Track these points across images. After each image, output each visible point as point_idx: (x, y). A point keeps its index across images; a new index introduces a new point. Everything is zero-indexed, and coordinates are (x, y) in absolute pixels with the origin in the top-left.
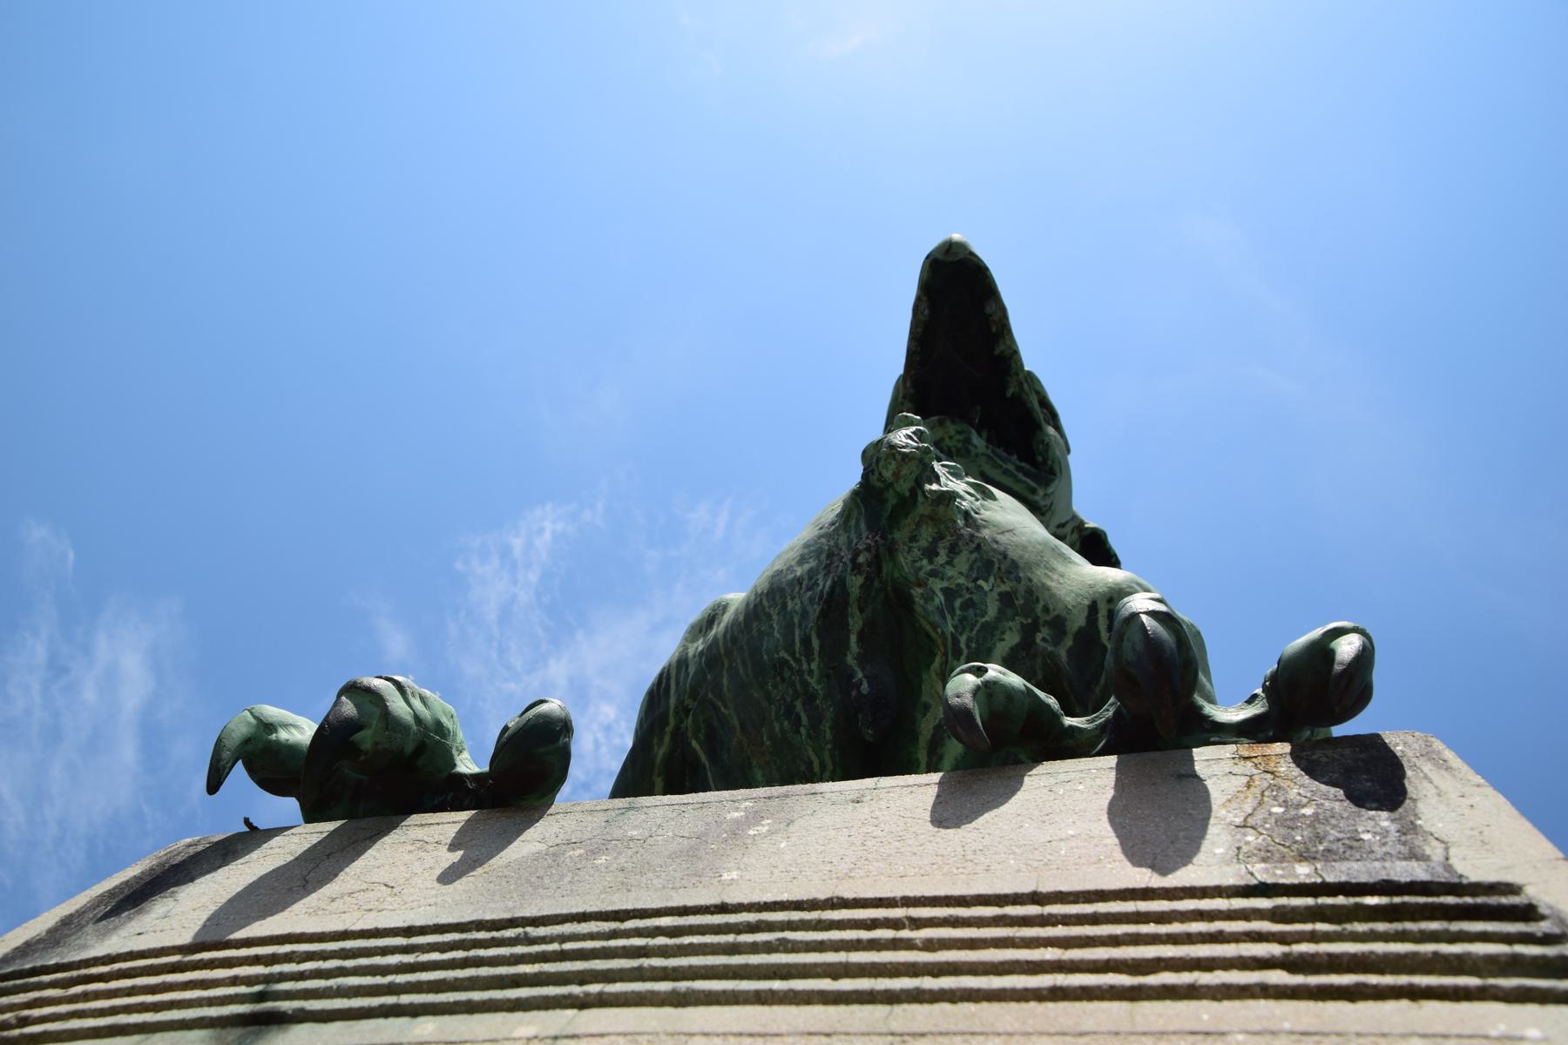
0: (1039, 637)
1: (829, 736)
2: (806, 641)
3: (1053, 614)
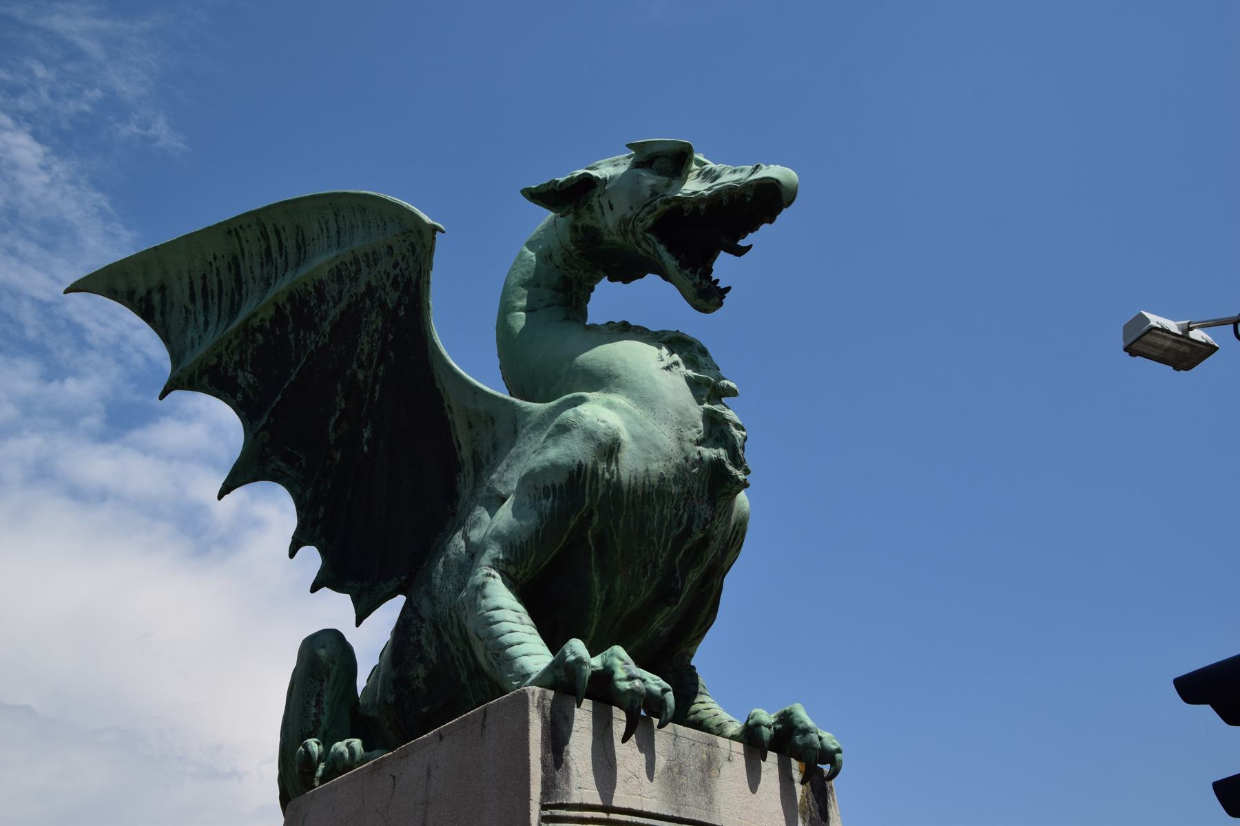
2: (666, 541)
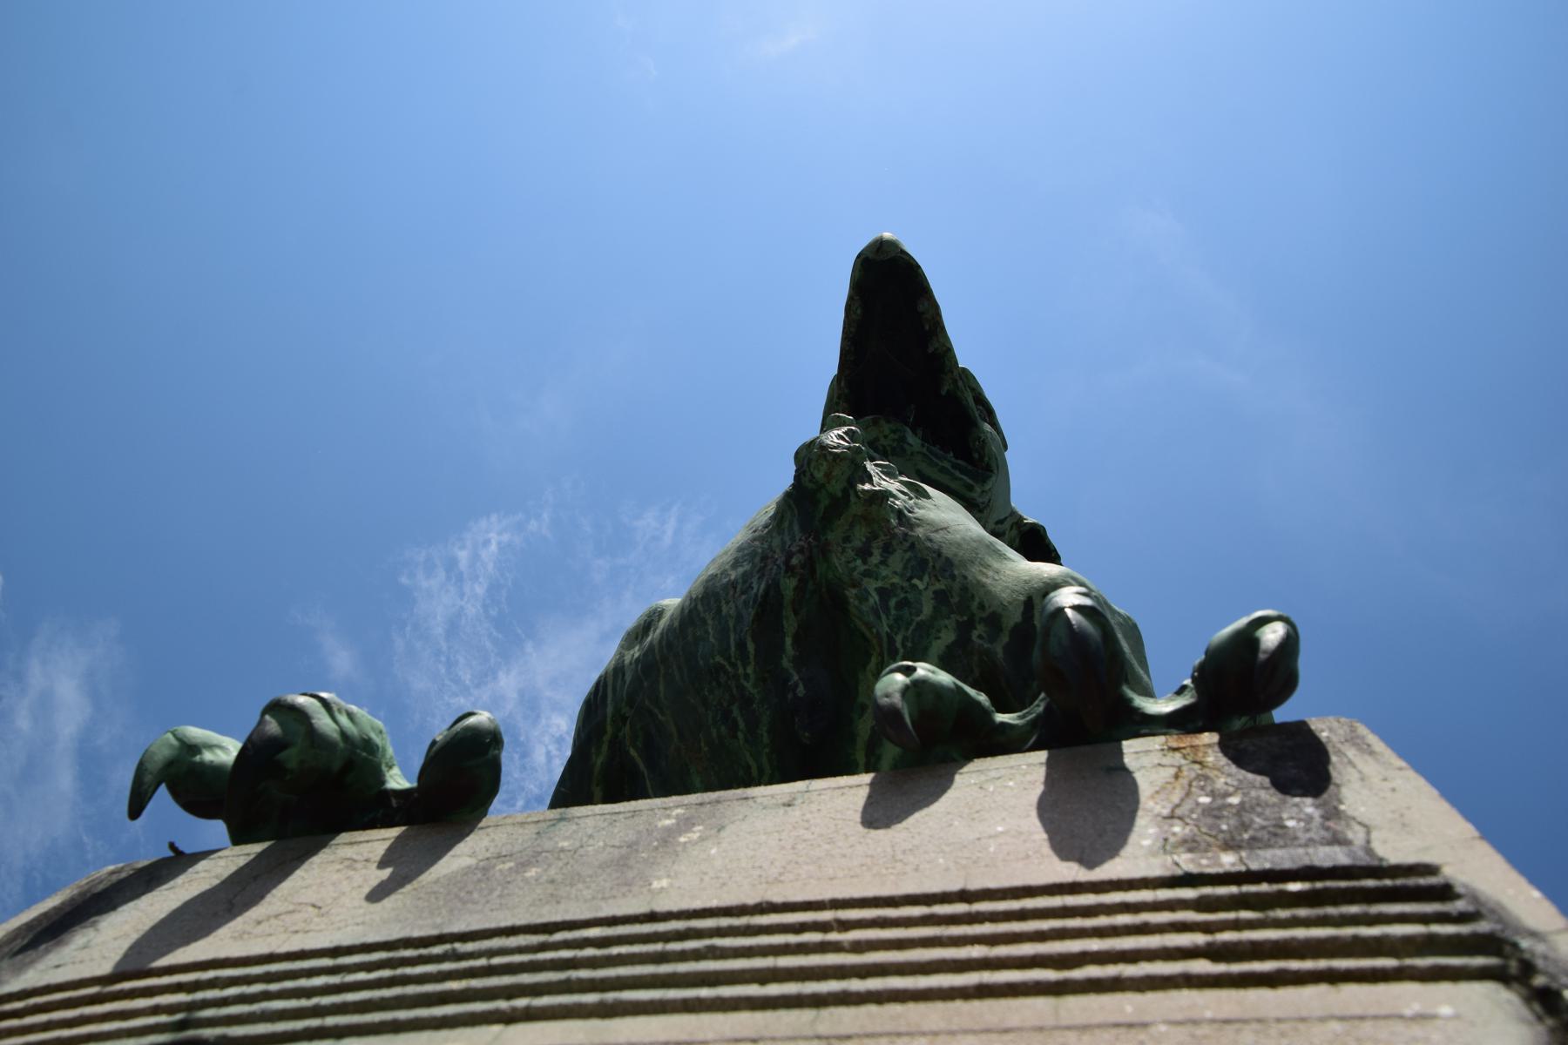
0: (975, 634)
1: (766, 740)
2: (741, 646)
3: (989, 611)
